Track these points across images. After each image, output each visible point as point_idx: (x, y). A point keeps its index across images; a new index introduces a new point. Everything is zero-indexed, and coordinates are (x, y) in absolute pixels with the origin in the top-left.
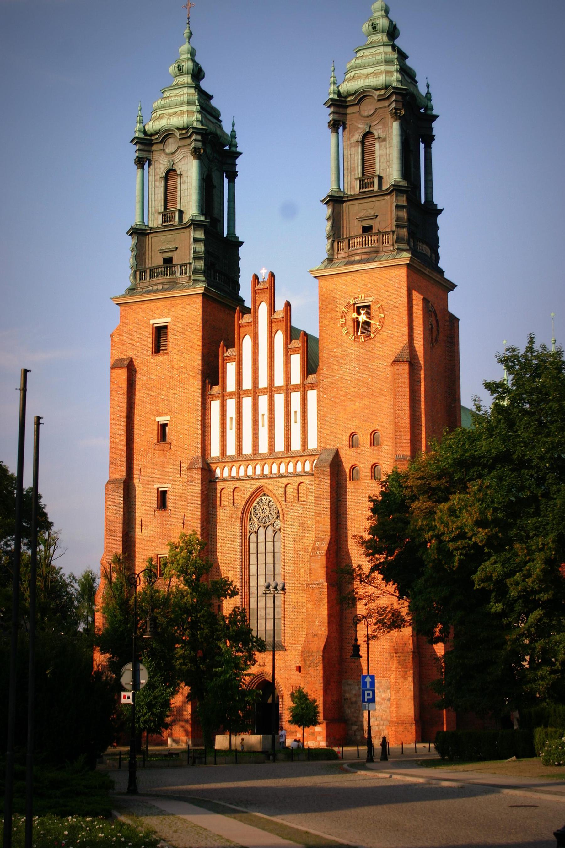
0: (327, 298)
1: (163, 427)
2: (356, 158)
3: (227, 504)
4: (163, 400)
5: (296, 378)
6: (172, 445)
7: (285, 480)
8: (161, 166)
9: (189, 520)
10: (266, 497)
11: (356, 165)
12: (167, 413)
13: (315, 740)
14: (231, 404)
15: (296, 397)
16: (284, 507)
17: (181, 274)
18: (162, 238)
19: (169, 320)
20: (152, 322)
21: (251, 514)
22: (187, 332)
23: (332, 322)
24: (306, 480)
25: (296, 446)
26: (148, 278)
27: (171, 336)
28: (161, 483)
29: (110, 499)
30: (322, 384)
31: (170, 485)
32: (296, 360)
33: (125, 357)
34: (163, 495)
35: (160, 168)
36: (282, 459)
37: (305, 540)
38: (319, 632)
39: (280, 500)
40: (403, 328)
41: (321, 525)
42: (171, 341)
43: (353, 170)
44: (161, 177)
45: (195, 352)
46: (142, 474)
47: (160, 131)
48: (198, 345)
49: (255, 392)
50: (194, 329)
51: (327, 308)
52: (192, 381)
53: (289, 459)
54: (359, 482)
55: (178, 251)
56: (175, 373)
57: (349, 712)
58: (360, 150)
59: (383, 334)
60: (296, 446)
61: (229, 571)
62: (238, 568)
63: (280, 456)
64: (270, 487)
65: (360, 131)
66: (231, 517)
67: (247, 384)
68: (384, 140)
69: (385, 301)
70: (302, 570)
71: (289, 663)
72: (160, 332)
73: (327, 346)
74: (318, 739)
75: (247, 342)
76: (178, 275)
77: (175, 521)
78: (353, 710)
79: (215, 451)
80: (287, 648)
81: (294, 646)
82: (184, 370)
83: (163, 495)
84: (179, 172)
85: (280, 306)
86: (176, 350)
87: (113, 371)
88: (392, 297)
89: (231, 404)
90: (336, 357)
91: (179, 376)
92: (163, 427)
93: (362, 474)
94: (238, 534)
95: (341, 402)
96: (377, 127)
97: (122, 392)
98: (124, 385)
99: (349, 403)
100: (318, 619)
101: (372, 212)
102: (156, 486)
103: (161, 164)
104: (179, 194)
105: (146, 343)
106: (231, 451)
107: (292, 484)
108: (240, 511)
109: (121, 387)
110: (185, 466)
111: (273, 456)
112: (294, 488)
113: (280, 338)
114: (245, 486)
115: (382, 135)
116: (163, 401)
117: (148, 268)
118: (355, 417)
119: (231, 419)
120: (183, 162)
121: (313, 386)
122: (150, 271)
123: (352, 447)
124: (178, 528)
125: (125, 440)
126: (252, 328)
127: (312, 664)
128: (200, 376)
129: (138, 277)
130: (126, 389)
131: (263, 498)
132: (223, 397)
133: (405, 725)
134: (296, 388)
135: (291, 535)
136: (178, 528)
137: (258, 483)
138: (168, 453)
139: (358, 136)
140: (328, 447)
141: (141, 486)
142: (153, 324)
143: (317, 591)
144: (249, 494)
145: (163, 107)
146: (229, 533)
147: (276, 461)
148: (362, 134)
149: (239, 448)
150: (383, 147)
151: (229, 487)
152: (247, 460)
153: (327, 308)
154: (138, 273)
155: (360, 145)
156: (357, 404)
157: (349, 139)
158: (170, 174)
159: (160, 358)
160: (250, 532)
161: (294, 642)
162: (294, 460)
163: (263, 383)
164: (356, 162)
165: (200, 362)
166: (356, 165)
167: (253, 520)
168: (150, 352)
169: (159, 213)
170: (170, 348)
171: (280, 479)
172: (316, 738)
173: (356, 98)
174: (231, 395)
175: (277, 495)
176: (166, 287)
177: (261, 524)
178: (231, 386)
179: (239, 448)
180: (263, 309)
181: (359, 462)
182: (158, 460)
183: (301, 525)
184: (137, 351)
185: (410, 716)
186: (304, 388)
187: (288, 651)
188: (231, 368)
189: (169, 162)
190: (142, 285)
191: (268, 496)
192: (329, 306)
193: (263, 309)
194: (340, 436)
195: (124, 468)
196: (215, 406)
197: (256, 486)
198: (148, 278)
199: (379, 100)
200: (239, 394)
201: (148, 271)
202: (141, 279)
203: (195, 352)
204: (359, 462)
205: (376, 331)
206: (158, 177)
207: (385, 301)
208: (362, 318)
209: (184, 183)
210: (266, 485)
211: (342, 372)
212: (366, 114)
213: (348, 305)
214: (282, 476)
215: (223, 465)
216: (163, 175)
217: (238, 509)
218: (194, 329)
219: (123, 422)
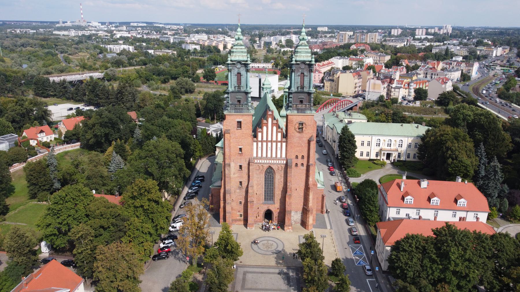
1: (241, 149)
14: (260, 144)
15: (279, 144)
18: (237, 94)
43: (297, 83)
49: (267, 141)
59: (306, 132)
67: (265, 139)
72: (239, 123)
75: (265, 128)
79: (255, 155)
83: (241, 167)
89: (260, 144)
92: (241, 149)
103: (235, 71)
106: (260, 155)
110: (248, 160)
113: (275, 128)
121: (284, 142)
132: (257, 142)
134: (279, 142)
139: (299, 73)
149: (262, 155)
152: (264, 159)
163: (270, 139)
179: (262, 155)
188: (260, 135)
200: (262, 141)
208: (301, 127)
214: (275, 164)
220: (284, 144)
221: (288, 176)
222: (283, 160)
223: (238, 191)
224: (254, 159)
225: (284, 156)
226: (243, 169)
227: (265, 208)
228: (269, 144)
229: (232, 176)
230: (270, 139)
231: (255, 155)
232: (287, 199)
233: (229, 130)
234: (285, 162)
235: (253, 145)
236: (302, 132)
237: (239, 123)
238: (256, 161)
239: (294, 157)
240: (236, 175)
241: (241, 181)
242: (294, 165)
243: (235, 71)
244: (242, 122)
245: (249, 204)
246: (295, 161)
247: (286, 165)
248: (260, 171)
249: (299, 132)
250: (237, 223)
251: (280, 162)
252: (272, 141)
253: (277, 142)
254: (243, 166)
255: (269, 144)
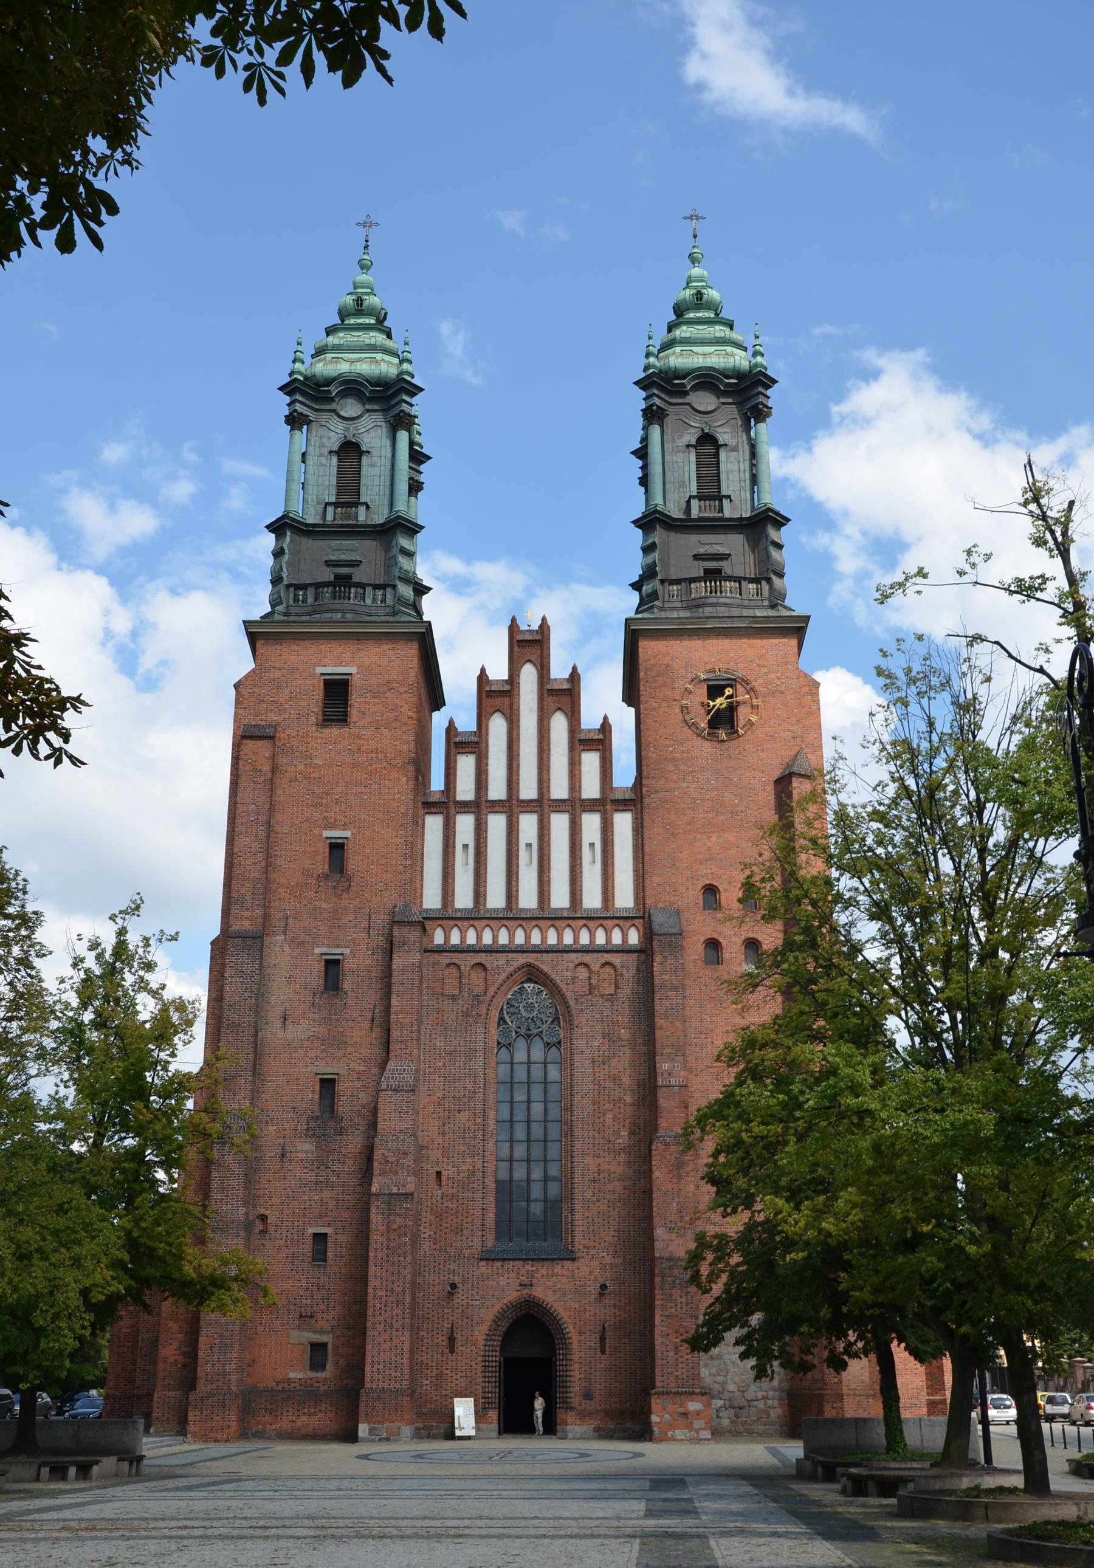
0: (654, 666)
1: (337, 848)
2: (686, 468)
3: (456, 992)
4: (337, 802)
5: (591, 789)
6: (356, 879)
7: (573, 956)
8: (332, 434)
9: (396, 1014)
10: (532, 985)
11: (687, 479)
12: (345, 825)
13: (689, 1427)
15: (591, 823)
16: (572, 1003)
17: (374, 600)
18: (335, 543)
19: (353, 670)
20: (320, 670)
21: (502, 1009)
22: (388, 694)
23: (664, 704)
24: (616, 959)
25: (592, 899)
26: (310, 600)
27: (356, 700)
28: (329, 946)
29: (232, 964)
30: (646, 801)
31: (347, 951)
32: (590, 761)
33: (263, 723)
34: (332, 966)
35: (329, 438)
36: (570, 922)
37: (614, 1062)
38: (679, 1224)
39: (564, 990)
40: (793, 725)
41: (668, 1033)
42: (357, 705)
44: (330, 452)
45: (404, 728)
46: (290, 927)
47: (334, 379)
48: (409, 717)
49: (512, 806)
50: (402, 690)
51: (655, 681)
52: (395, 775)
53: (584, 921)
54: (720, 967)
55: (362, 567)
56: (362, 758)
57: (707, 1373)
58: (693, 457)
59: (760, 733)
60: (592, 899)
61: (459, 1112)
62: (479, 1107)
63: (565, 914)
64: (545, 968)
65: (693, 430)
66: (467, 1015)
67: (497, 790)
68: (735, 449)
69: (760, 681)
70: (610, 1115)
71: (582, 1283)
72: (337, 692)
73: (656, 740)
74: (696, 1426)
75: (498, 726)
76: (368, 601)
77: (355, 1015)
78: (713, 1371)
79: (432, 899)
80: (578, 1255)
81: (593, 1252)
82: (381, 756)
84: (364, 448)
85: (559, 671)
86: (365, 721)
87: (245, 741)
88: (773, 676)
90: (674, 760)
91: (371, 764)
93: (726, 956)
94: (480, 1045)
95: (684, 833)
96: (720, 430)
97: (262, 779)
98: (266, 768)
99: (699, 836)
100: (677, 1199)
101: (721, 550)
102: (317, 951)
104: (363, 481)
105: (306, 703)
106: (464, 899)
107: (586, 965)
108: (484, 1007)
109: (260, 771)
110: (380, 920)
111: (544, 916)
112: (590, 971)
113: (559, 724)
114: (496, 963)
115: (732, 442)
116: (337, 803)
117: (311, 585)
118: (710, 859)
119: (465, 846)
120: (373, 433)
122: (316, 588)
123: (705, 909)
124: (361, 1028)
125: (263, 863)
126: (507, 701)
127: (678, 1282)
128: (411, 768)
129: (292, 596)
130: (269, 775)
131: (526, 985)
133: (858, 1398)
134: (592, 806)
135: (587, 1052)
136: (361, 1028)
137: (522, 959)
138: (345, 895)
140: (660, 905)
141: (287, 948)
142: (322, 674)
143: (673, 1148)
144: (503, 976)
145: (338, 348)
146: (462, 1043)
147: (558, 923)
148: (697, 436)
149: (479, 893)
150: (732, 459)
151: (466, 961)
152: (497, 919)
153: (655, 681)
154: (292, 589)
155: (693, 450)
156: (714, 839)
157: (673, 441)
158: (350, 452)
159: (334, 732)
160: (499, 1043)
161: (592, 1244)
162: (591, 924)
163: (528, 790)
164: (687, 474)
165: (412, 745)
166: (687, 479)
167: (505, 1022)
168: (313, 720)
169: (327, 504)
170: (354, 715)
171: (564, 955)
172: (692, 1423)
173: (689, 382)
174: (465, 807)
175: (558, 981)
176: (349, 616)
177: (523, 1031)
178: (465, 790)
180: (528, 674)
181: (720, 934)
182: (324, 905)
183: (604, 1036)
184: (287, 715)
185: (863, 1382)
186: (608, 804)
187: (582, 1260)
189: (347, 429)
190: (298, 610)
191: (536, 982)
192: (660, 679)
193: (528, 674)
194: (682, 889)
195: (258, 912)
196: (434, 824)
197: (516, 964)
198: (310, 600)
199: (725, 394)
200: (480, 806)
201: (311, 592)
202: (296, 600)
203: (404, 728)
204: (720, 934)
205: (745, 726)
206: (326, 451)
207: (760, 681)
209: (373, 465)
210: (536, 963)
211: (685, 785)
212: (702, 409)
213: (695, 680)
214: (567, 950)
215: (452, 923)
216: (335, 448)
217: (483, 1002)
218: (402, 690)
219: (261, 831)
220: (623, 822)
221: (660, 1007)
222: (623, 919)
223: (305, 1147)
224: (425, 922)
225: (625, 898)
226: (347, 984)
227: (500, 1288)
228: (528, 824)
229: (273, 1033)
230: (528, 790)
231: (432, 899)
232: (658, 1174)
233: (275, 727)
234: (634, 938)
235: (419, 828)
236: (733, 731)
237: (337, 692)
238: (439, 938)
239: (694, 895)
240: (296, 1032)
241: (331, 1069)
242: (695, 949)
243: (333, 433)
244: (356, 682)
245: (377, 1219)
246: (700, 926)
247: (645, 951)
248: (461, 1005)
249: (712, 736)
250: (283, 1423)
251: (600, 938)
252: (542, 806)
253: (575, 806)
254: (347, 965)
255: (528, 824)
